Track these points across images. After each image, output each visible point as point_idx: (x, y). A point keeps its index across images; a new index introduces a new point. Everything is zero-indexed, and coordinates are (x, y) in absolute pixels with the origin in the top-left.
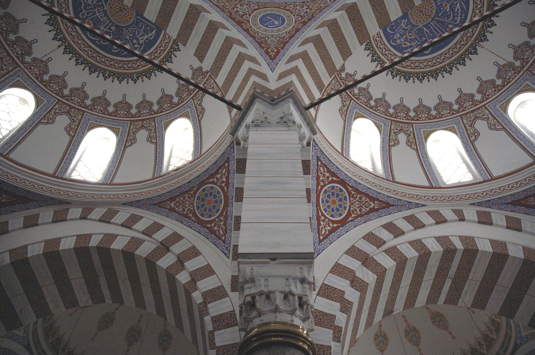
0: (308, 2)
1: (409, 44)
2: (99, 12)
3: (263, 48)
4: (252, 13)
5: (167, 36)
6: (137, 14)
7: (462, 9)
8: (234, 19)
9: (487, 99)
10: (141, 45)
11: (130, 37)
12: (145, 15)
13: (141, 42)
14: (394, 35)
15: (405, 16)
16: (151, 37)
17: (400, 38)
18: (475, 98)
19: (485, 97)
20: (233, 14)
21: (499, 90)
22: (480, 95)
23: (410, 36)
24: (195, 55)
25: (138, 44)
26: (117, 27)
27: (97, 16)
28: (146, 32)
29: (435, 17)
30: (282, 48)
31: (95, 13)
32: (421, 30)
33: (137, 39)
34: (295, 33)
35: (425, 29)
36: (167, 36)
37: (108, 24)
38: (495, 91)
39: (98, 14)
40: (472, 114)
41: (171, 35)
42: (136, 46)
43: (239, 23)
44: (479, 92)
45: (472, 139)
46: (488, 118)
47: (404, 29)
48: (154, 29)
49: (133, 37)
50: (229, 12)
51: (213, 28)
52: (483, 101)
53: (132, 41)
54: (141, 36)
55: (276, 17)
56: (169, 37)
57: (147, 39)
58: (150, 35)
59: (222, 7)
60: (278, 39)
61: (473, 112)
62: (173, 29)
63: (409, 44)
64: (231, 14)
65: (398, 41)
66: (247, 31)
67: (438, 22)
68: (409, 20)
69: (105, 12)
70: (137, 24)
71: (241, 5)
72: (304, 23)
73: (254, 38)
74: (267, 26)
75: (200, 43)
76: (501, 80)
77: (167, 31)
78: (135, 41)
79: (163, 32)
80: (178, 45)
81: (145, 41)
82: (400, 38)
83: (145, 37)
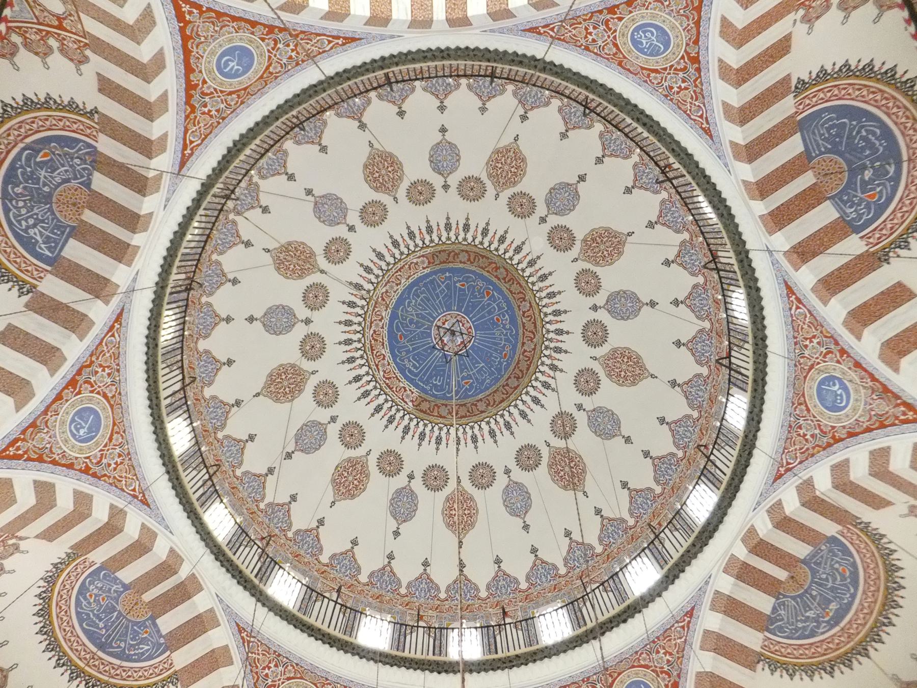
0: (130, 459)
1: (92, 601)
2: (66, 171)
3: (24, 432)
4: (98, 393)
5: (42, 275)
6: (73, 228)
7: (143, 654)
8: (79, 372)
10: (26, 231)
11: (37, 214)
12: (72, 241)
13: (31, 232)
14: (99, 580)
15: (126, 587)
16: (40, 248)
17: (97, 587)
20: (88, 370)
23: (103, 599)
24: (9, 324)
25: (28, 227)
26: (50, 195)
27: (58, 168)
28: (47, 240)
29: (133, 622)
30: (29, 459)
31: (63, 166)
32: (113, 609)
33: (34, 226)
34: (63, 465)
35: (116, 614)
36: (42, 275)
37: (51, 182)
39: (63, 169)
41: (44, 281)
42: (24, 223)
43: (72, 383)
47: (110, 589)
48: (52, 253)
49: (37, 219)
50: (92, 362)
51: (47, 355)
53: (31, 217)
54: (40, 232)
55: (95, 427)
56: (41, 278)
57: (37, 241)
58: (43, 246)
59: (100, 350)
60: (48, 446)
62: (53, 287)
63: (92, 601)
64: (89, 366)
65: (91, 587)
66: (59, 397)
67: (127, 627)
68: (122, 592)
69: (67, 181)
70: (58, 227)
71: (109, 374)
72: (86, 471)
73: (45, 412)
74: (73, 421)
75: (27, 333)
77: (49, 276)
78: (31, 222)
79: (49, 268)
80: (28, 292)
81: (32, 238)
82: (97, 587)
83: (38, 238)
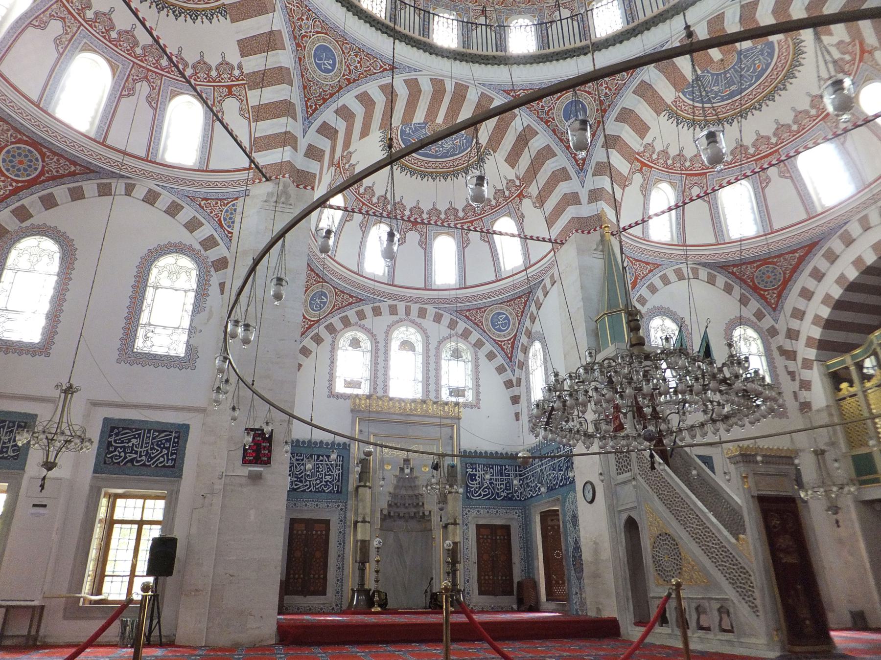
9: (91, 26)
18: (87, 11)
19: (92, 23)
21: (104, 37)
22: (93, 17)
38: (103, 33)
40: (66, 12)
44: (96, 14)
45: (34, 22)
46: (67, 34)
52: (86, 22)
61: (70, 13)
76: (116, 36)
